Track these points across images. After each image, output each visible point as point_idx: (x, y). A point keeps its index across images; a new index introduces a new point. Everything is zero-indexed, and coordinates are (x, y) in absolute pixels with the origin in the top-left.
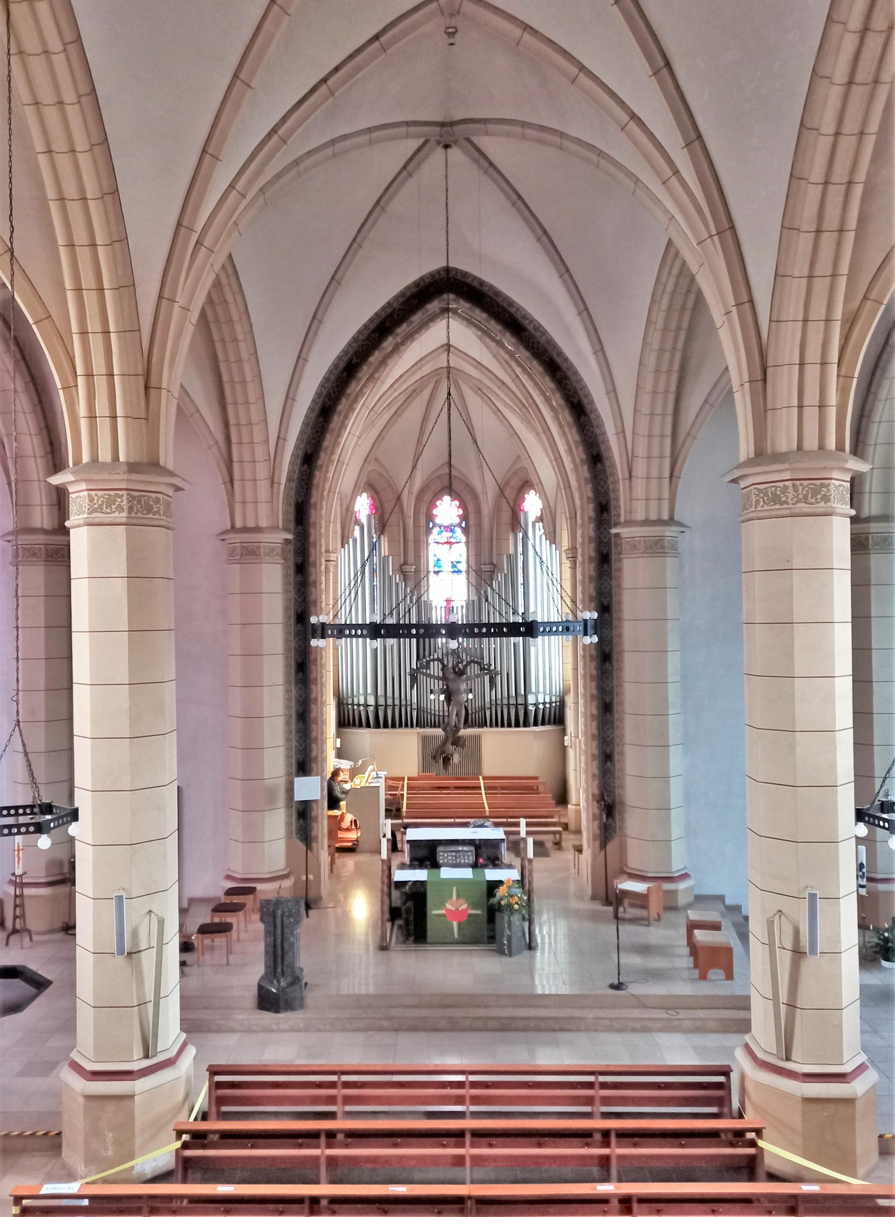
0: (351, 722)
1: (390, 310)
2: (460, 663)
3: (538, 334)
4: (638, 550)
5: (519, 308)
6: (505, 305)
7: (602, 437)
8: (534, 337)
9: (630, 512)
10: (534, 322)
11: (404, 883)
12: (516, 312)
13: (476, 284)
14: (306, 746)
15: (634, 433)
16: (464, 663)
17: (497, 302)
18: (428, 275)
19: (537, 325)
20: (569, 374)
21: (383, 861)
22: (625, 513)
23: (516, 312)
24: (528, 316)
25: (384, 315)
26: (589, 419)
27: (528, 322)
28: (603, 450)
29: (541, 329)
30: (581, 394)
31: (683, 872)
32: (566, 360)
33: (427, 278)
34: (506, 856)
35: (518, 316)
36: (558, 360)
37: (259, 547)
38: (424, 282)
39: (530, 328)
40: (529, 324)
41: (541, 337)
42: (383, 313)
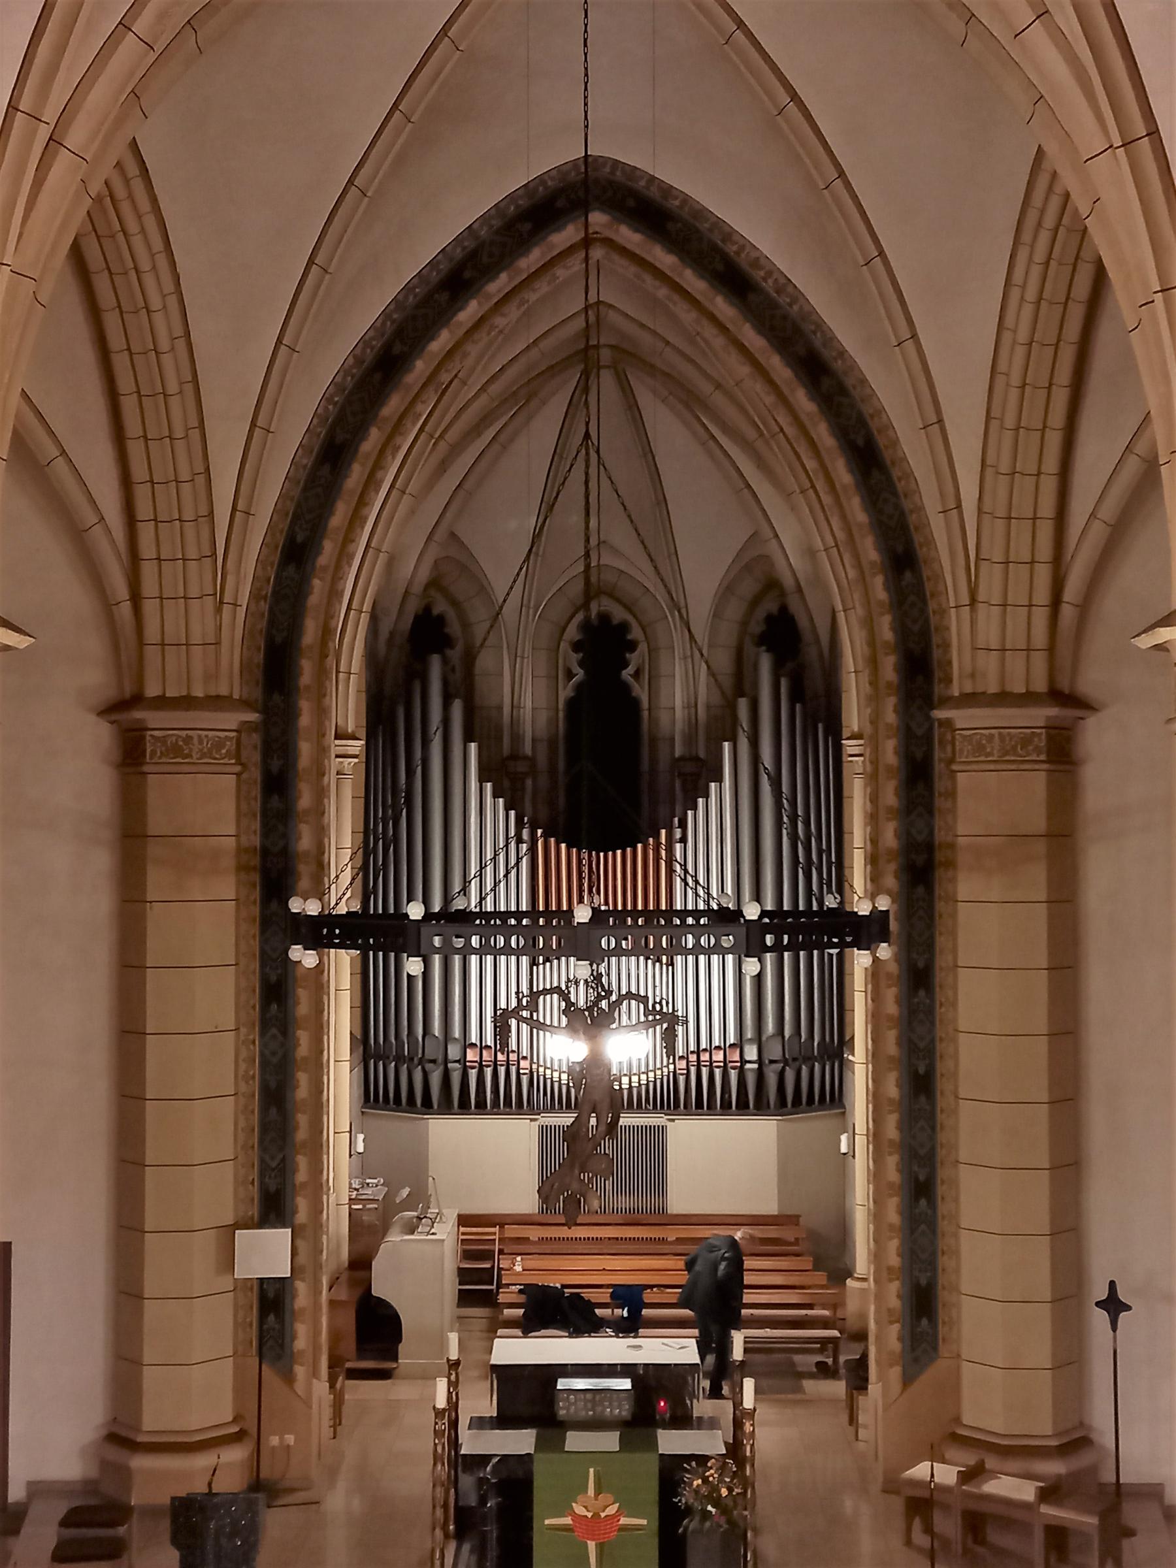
0: (391, 1095)
1: (470, 244)
2: (604, 998)
3: (783, 300)
4: (988, 755)
5: (745, 244)
6: (717, 238)
7: (914, 516)
8: (774, 305)
9: (973, 676)
10: (775, 276)
11: (484, 1459)
12: (738, 253)
13: (654, 193)
14: (283, 1160)
15: (980, 511)
16: (614, 998)
17: (698, 231)
18: (554, 172)
19: (782, 281)
20: (849, 382)
21: (439, 1413)
22: (960, 677)
23: (738, 253)
24: (763, 261)
25: (459, 253)
26: (889, 478)
27: (762, 273)
28: (917, 545)
29: (790, 289)
30: (874, 425)
31: (1076, 1435)
32: (842, 353)
33: (552, 179)
34: (702, 1407)
35: (743, 261)
36: (827, 354)
37: (188, 739)
38: (546, 188)
39: (769, 286)
40: (765, 279)
41: (790, 305)
42: (459, 250)
